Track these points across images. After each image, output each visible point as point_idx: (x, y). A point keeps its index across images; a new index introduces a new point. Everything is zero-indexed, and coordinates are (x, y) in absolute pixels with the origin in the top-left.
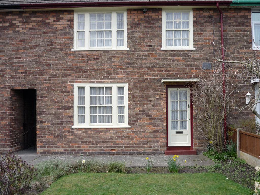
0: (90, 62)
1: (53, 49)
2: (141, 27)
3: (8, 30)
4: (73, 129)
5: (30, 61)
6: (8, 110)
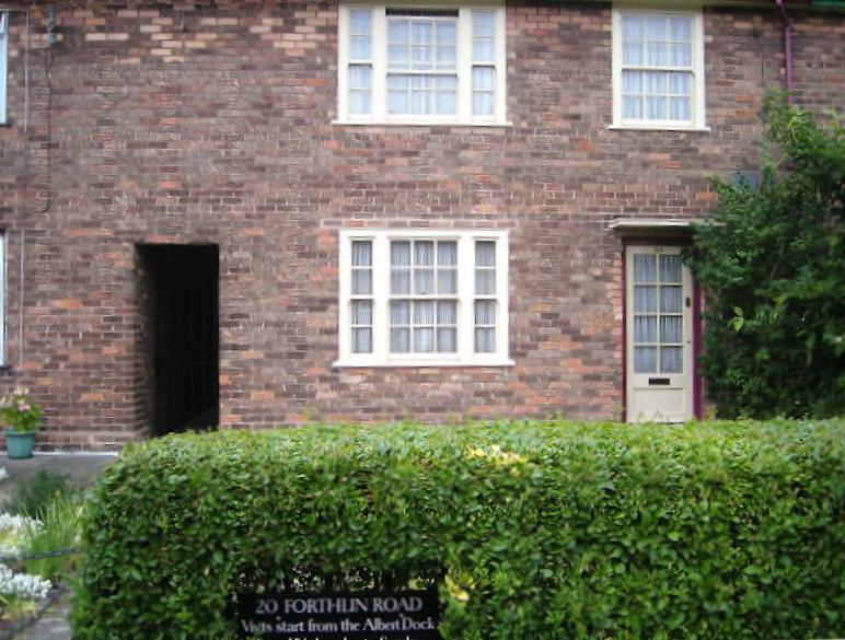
0: (389, 161)
1: (272, 120)
2: (549, 56)
3: (127, 56)
4: (336, 370)
5: (196, 150)
6: (127, 311)
